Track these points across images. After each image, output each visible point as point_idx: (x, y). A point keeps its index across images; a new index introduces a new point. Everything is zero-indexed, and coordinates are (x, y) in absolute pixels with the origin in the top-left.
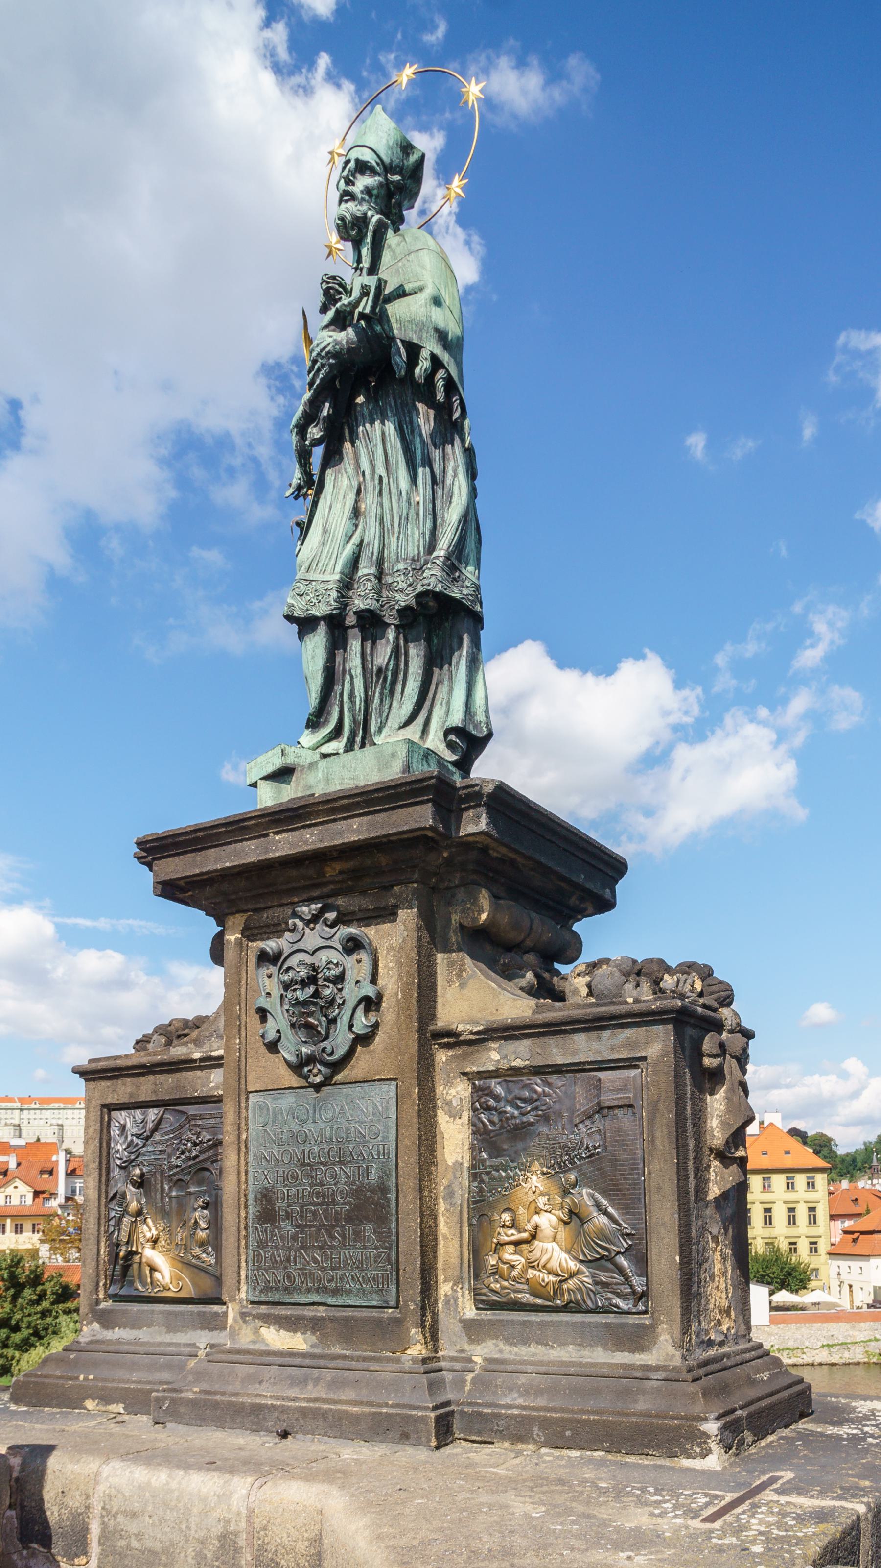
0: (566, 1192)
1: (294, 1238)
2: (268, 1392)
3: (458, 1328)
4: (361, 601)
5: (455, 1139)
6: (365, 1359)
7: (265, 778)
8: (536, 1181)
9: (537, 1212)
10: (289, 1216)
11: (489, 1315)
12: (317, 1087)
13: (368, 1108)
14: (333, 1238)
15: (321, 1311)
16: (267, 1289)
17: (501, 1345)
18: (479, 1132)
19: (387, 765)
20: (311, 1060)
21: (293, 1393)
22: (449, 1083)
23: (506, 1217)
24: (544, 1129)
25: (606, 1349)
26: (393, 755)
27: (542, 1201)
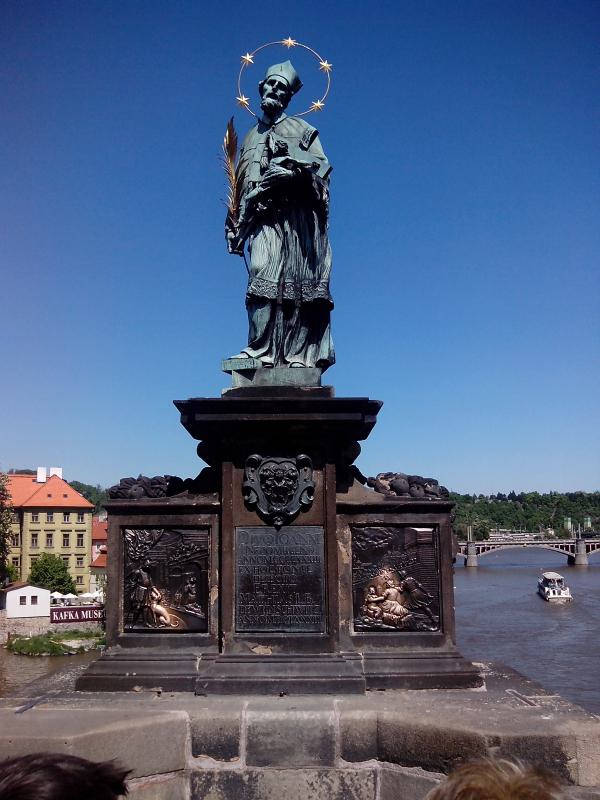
0: (401, 578)
1: (265, 599)
2: (263, 673)
3: (349, 640)
4: (289, 294)
5: (345, 554)
6: (311, 657)
7: (240, 371)
8: (386, 573)
9: (388, 587)
10: (261, 589)
11: (364, 634)
12: (278, 528)
13: (306, 538)
14: (288, 599)
15: (282, 635)
16: (248, 625)
17: (371, 646)
18: (355, 549)
19: (309, 378)
20: (274, 514)
21: (279, 675)
22: (343, 527)
23: (372, 589)
24: (389, 552)
25: (422, 645)
26: (313, 374)
27: (390, 582)
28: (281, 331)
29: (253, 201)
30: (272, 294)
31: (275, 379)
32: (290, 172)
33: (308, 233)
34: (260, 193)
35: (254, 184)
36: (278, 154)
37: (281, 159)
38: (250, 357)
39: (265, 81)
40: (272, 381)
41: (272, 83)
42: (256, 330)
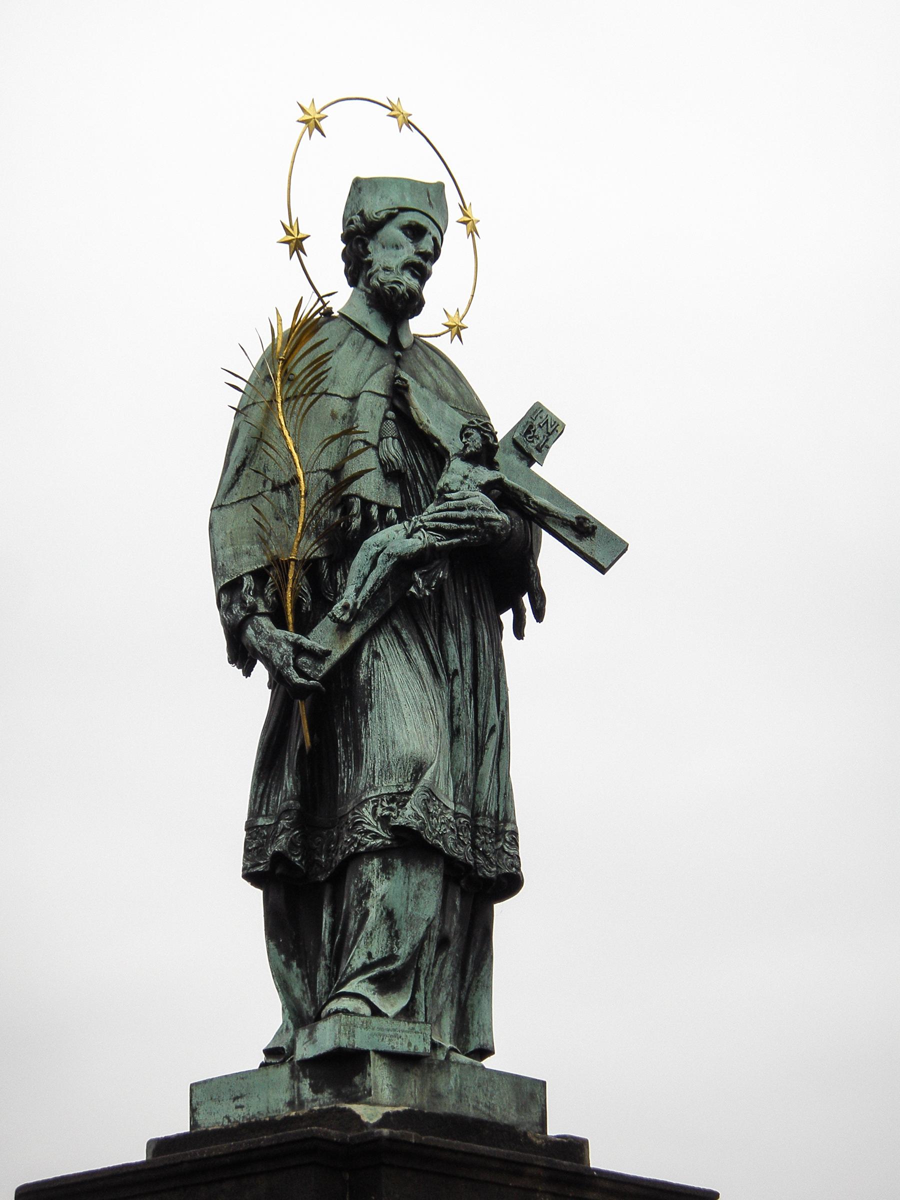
28: (433, 949)
29: (405, 565)
30: (450, 844)
31: (460, 1096)
32: (502, 516)
33: (493, 691)
34: (432, 547)
35: (366, 504)
36: (472, 458)
37: (485, 475)
38: (376, 1012)
39: (391, 217)
40: (452, 1099)
41: (416, 232)
42: (394, 936)
